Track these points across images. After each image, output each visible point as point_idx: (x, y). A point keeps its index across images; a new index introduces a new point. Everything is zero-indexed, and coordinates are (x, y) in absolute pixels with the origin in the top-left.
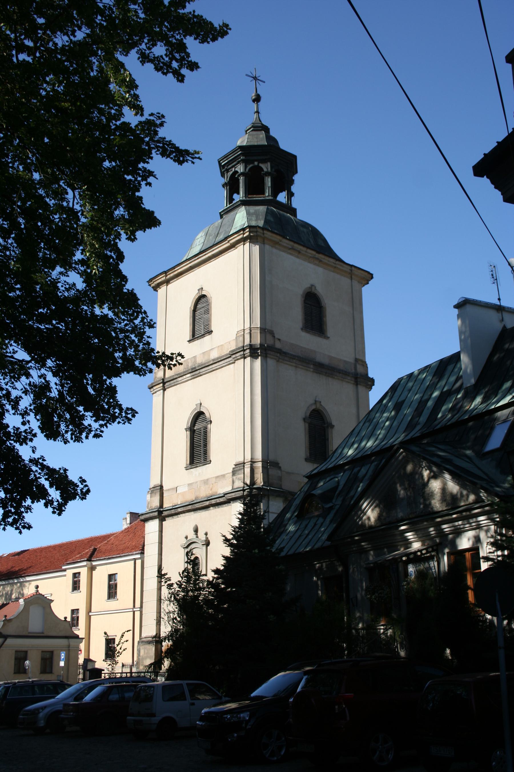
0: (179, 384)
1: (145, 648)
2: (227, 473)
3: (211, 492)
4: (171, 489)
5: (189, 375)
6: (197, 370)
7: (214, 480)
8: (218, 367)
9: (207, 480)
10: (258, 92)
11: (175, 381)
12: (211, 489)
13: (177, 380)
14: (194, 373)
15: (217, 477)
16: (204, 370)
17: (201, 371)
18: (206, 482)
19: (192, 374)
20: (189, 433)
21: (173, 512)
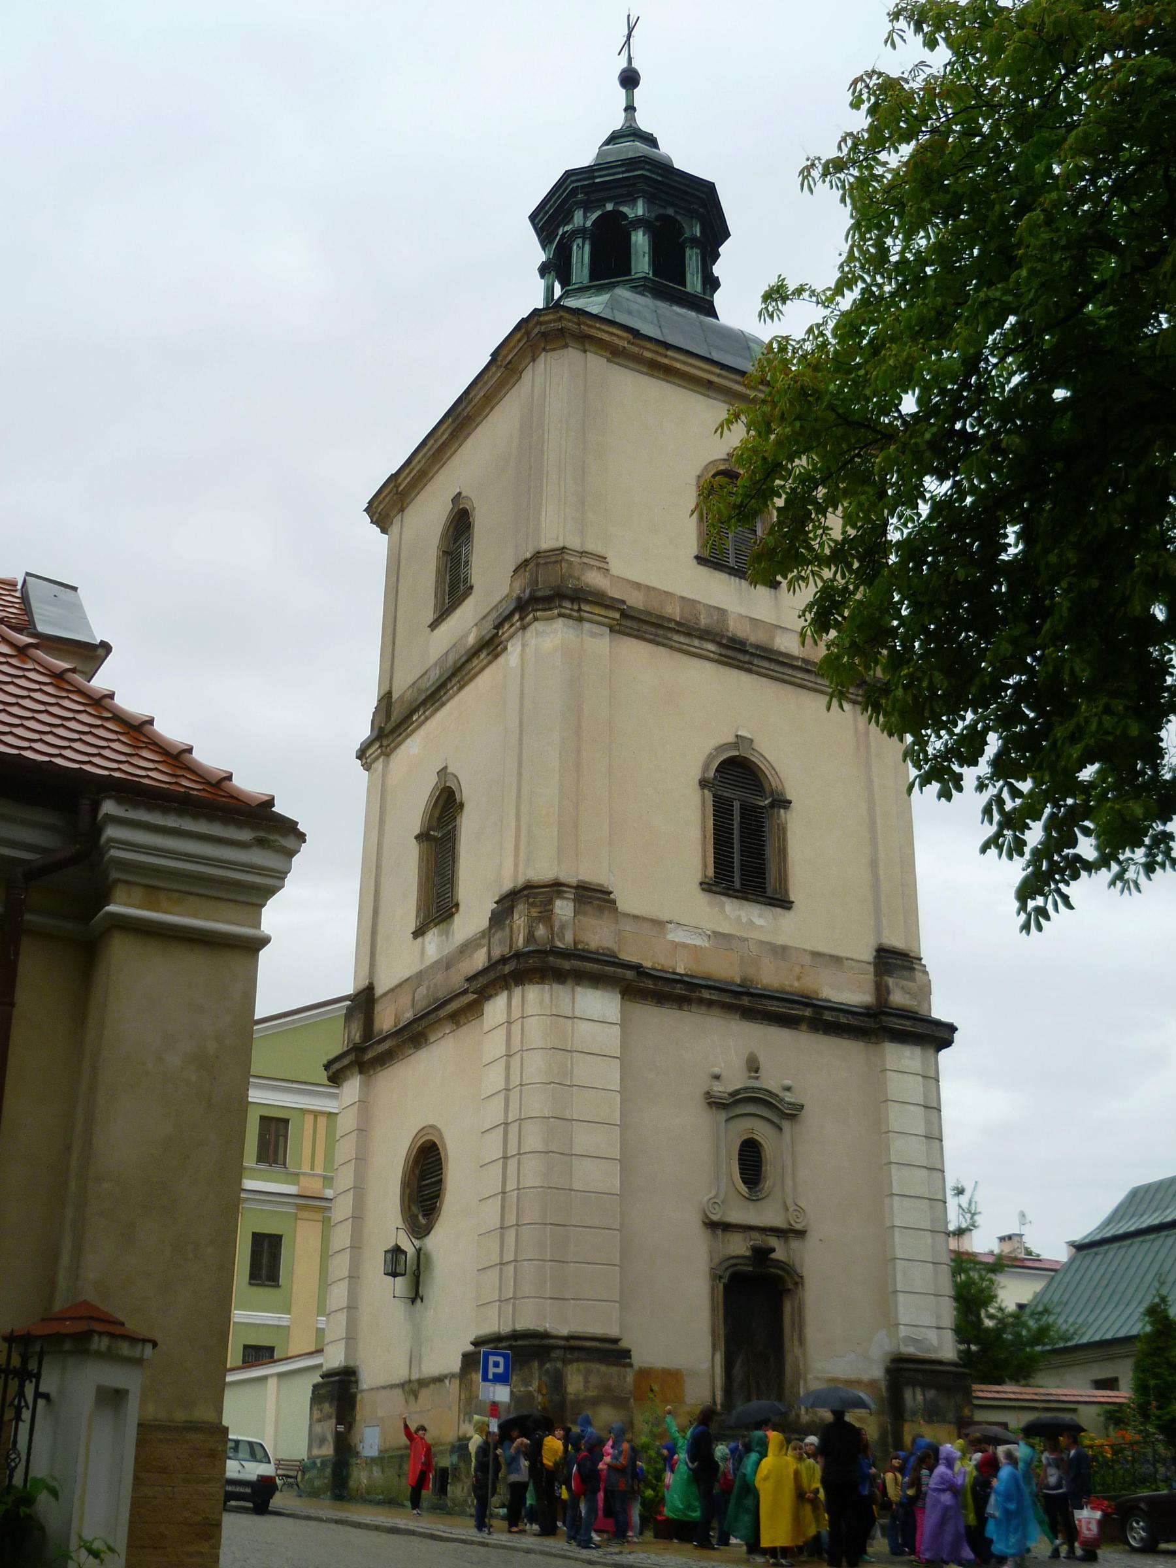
0: (671, 647)
1: (588, 1373)
2: (849, 955)
3: (796, 984)
4: (645, 919)
5: (711, 647)
6: (746, 652)
7: (807, 960)
8: (810, 684)
9: (784, 948)
10: (635, 64)
11: (660, 632)
12: (799, 978)
13: (669, 635)
14: (730, 653)
15: (816, 955)
16: (765, 664)
17: (756, 661)
18: (781, 952)
19: (724, 652)
20: (709, 795)
21: (679, 990)
